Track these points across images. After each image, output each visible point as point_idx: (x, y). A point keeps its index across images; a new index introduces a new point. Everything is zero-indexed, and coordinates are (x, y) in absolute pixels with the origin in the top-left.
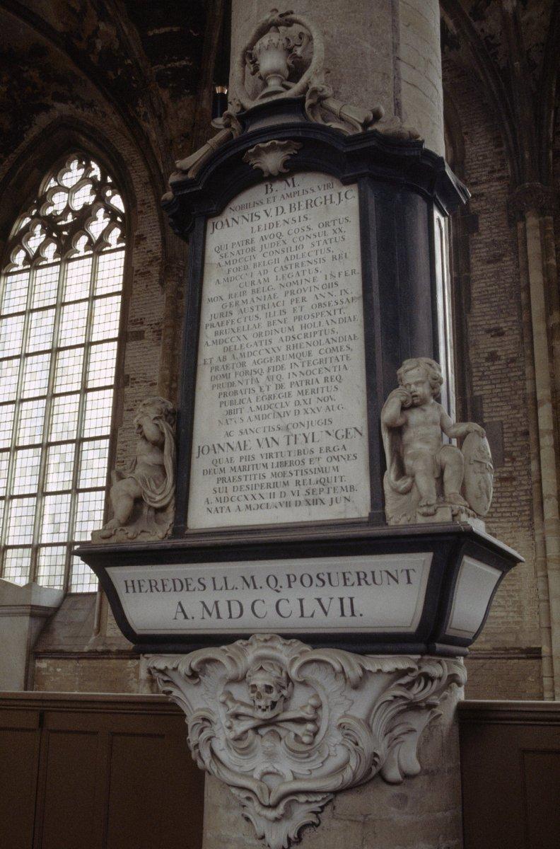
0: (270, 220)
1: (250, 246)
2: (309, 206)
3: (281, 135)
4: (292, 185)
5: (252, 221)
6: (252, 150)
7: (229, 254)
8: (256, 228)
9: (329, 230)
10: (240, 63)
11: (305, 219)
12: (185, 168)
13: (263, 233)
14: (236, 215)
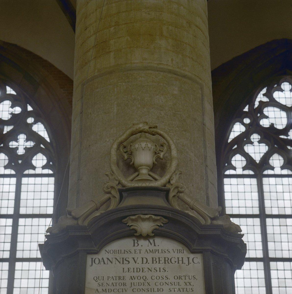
0: (136, 266)
1: (122, 281)
2: (166, 262)
3: (157, 213)
4: (153, 244)
5: (123, 263)
6: (133, 217)
7: (105, 284)
8: (126, 270)
9: (182, 282)
10: (115, 149)
11: (164, 271)
12: (77, 217)
13: (133, 274)
14: (110, 256)
